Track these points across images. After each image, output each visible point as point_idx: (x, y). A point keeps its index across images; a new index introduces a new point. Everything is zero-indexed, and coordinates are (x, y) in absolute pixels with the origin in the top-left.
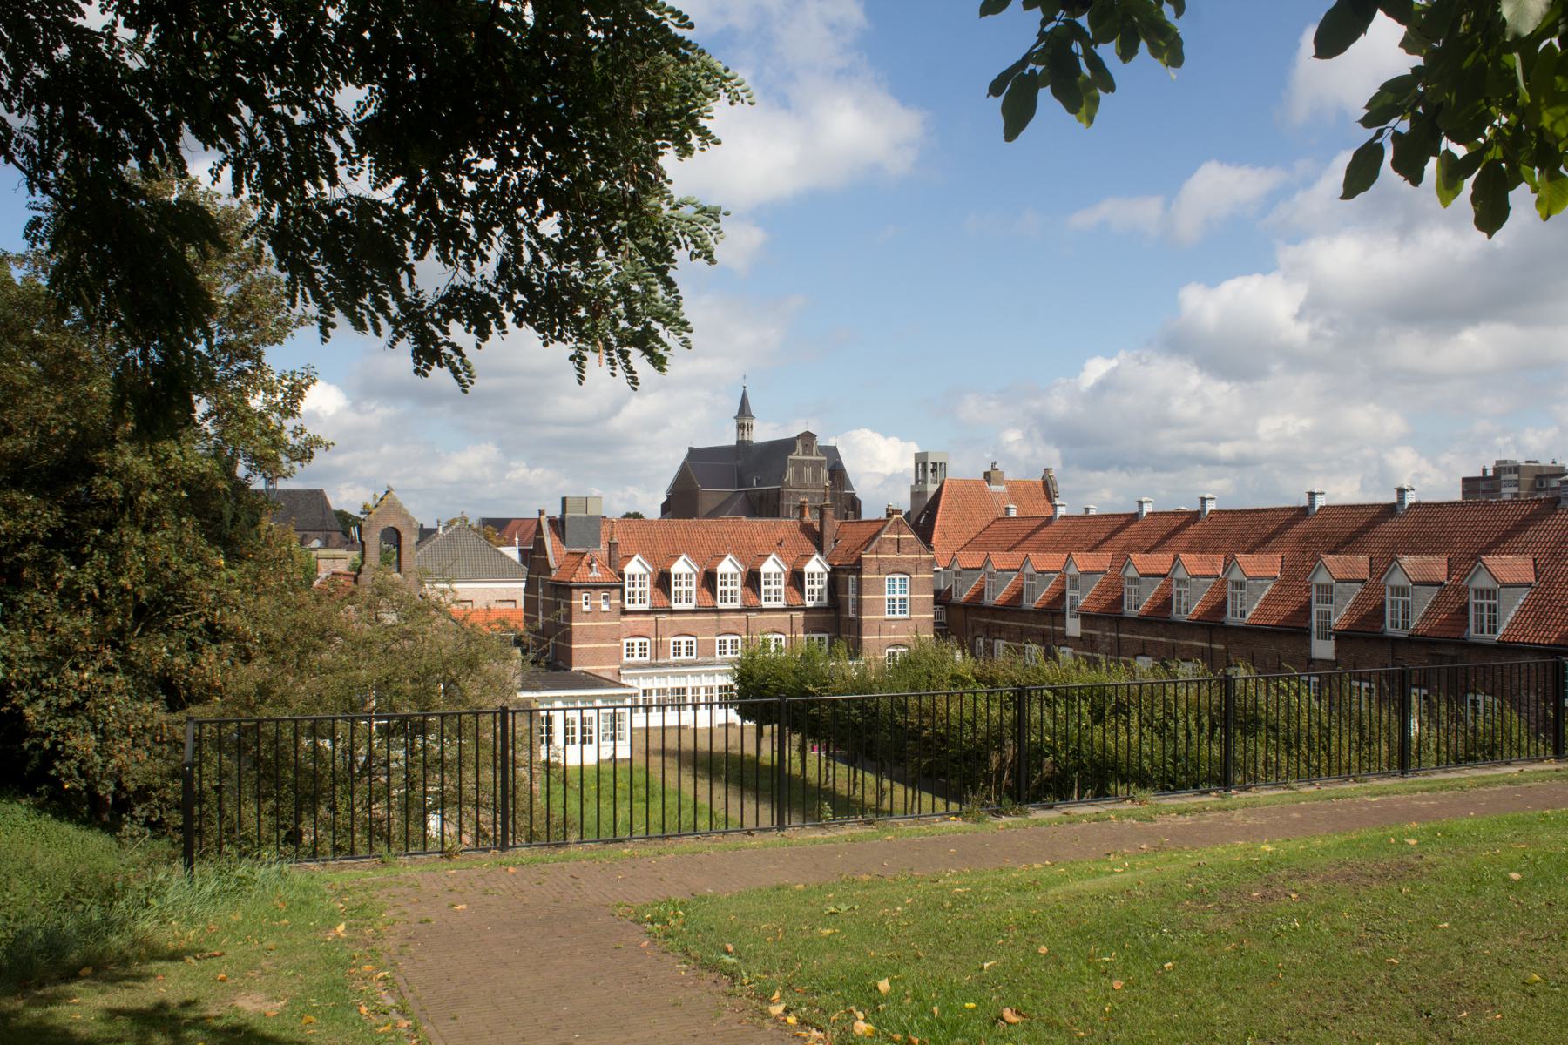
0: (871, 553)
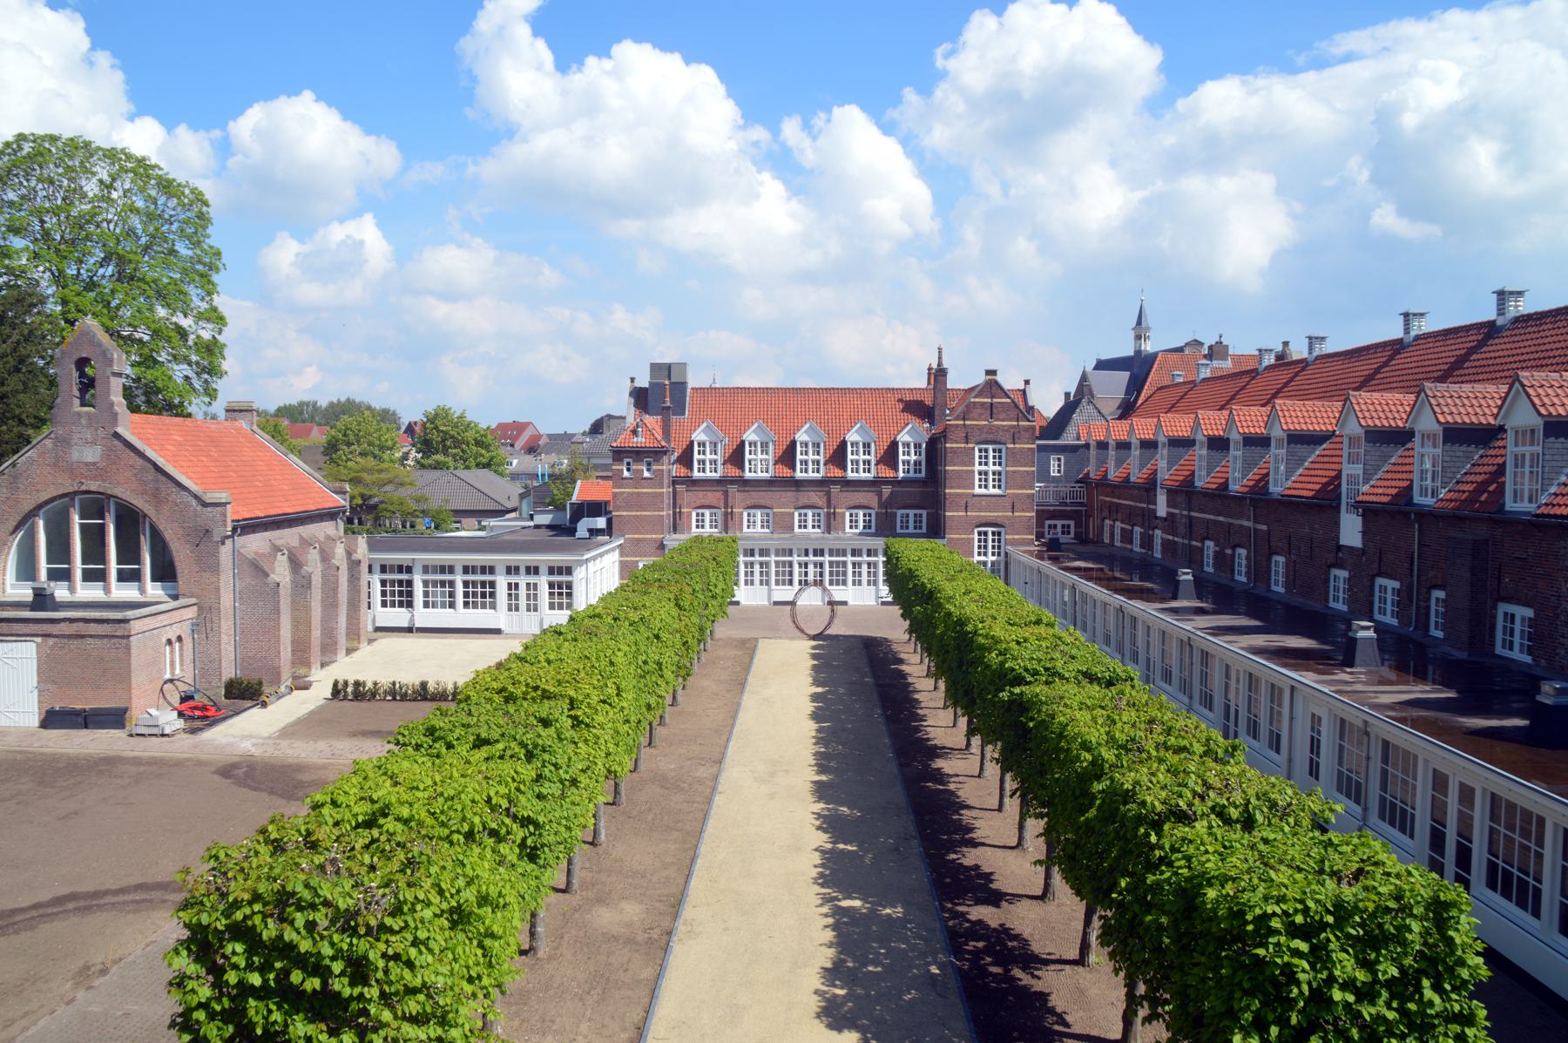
0: (957, 419)
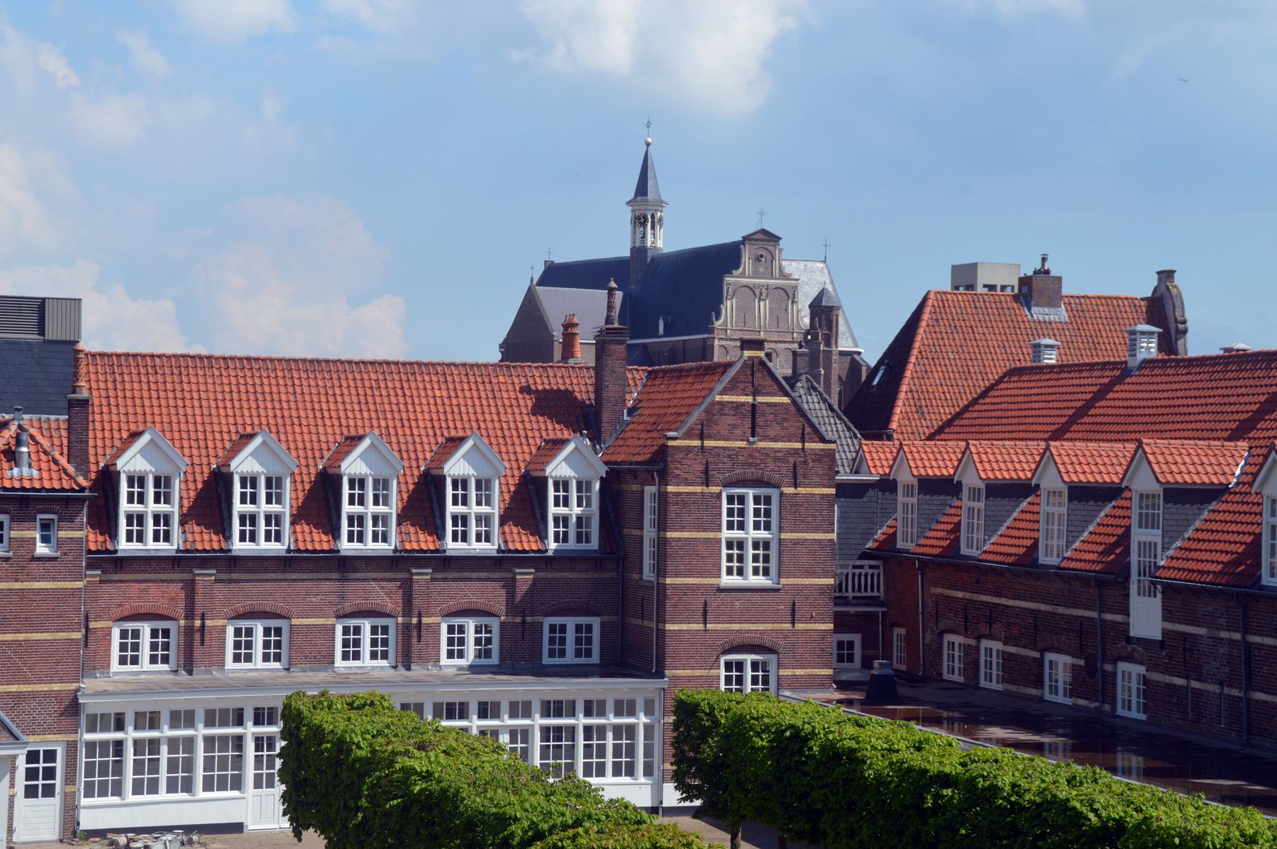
0: (688, 435)
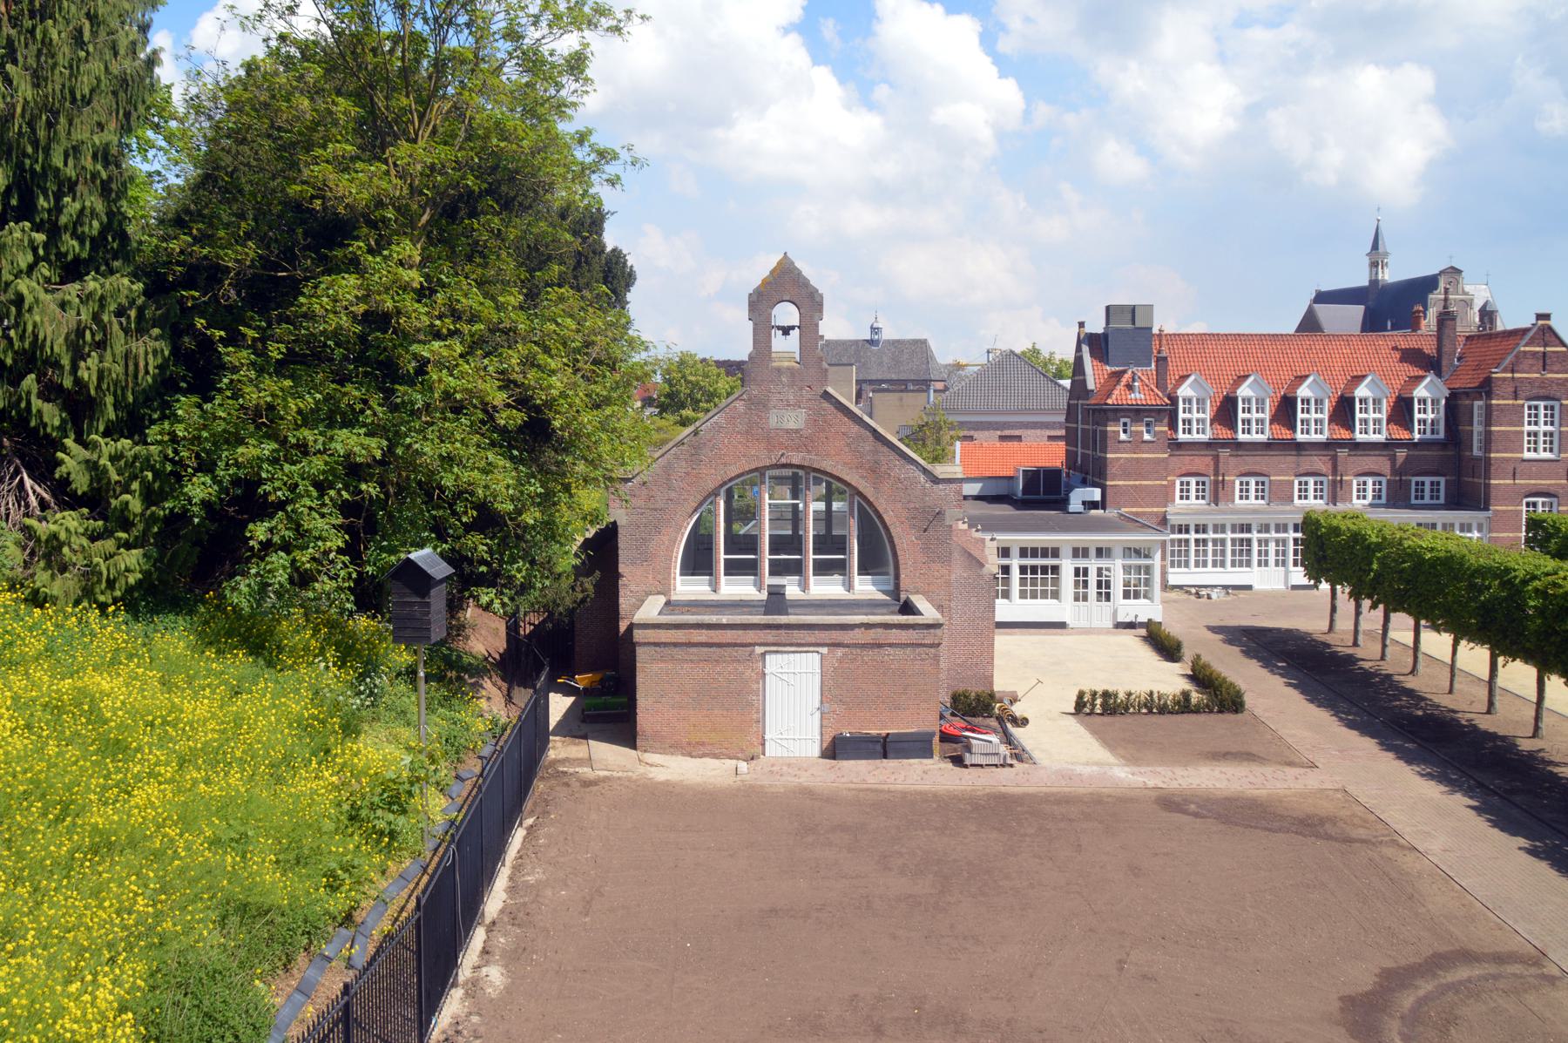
0: (1504, 371)
